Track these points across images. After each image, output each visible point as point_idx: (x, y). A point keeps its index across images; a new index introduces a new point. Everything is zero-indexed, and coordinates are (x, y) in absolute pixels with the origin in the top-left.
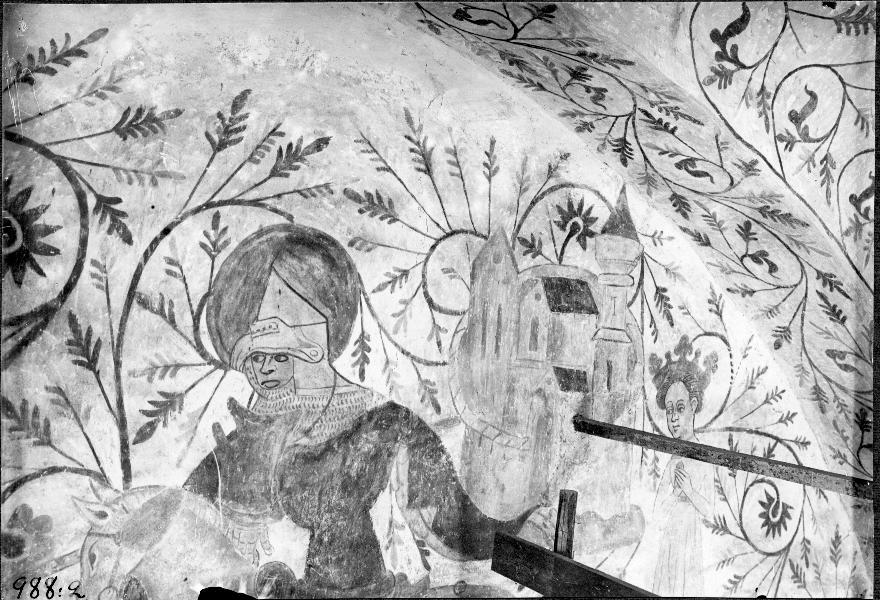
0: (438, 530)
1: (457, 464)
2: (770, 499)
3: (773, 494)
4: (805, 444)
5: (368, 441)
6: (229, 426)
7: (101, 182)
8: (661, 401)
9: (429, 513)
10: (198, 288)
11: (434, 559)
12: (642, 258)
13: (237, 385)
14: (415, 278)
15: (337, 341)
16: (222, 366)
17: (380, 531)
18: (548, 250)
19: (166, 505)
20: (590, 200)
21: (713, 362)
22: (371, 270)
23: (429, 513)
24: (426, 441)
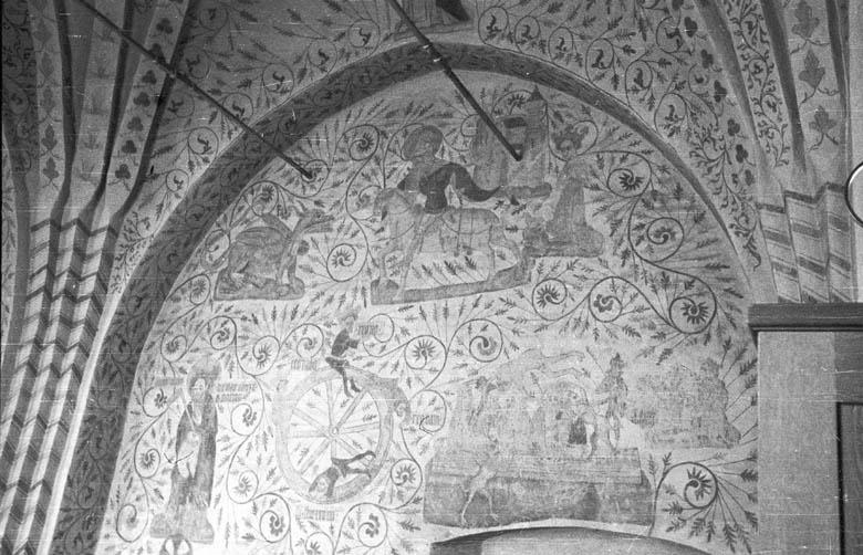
0: (465, 194)
1: (472, 176)
2: (627, 177)
3: (629, 174)
4: (649, 152)
5: (443, 173)
6: (407, 173)
7: (381, 129)
8: (558, 147)
9: (463, 190)
10: (402, 144)
11: (464, 202)
12: (546, 104)
13: (410, 164)
14: (458, 130)
15: (435, 150)
16: (407, 160)
17: (447, 195)
18: (505, 111)
19: (392, 191)
20: (521, 94)
21: (586, 131)
22: (445, 131)
23: (463, 190)
24: (462, 171)
